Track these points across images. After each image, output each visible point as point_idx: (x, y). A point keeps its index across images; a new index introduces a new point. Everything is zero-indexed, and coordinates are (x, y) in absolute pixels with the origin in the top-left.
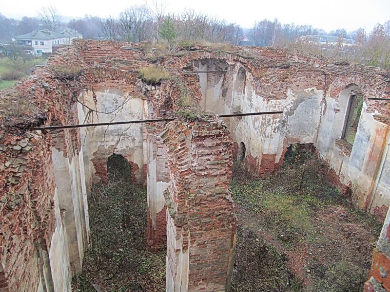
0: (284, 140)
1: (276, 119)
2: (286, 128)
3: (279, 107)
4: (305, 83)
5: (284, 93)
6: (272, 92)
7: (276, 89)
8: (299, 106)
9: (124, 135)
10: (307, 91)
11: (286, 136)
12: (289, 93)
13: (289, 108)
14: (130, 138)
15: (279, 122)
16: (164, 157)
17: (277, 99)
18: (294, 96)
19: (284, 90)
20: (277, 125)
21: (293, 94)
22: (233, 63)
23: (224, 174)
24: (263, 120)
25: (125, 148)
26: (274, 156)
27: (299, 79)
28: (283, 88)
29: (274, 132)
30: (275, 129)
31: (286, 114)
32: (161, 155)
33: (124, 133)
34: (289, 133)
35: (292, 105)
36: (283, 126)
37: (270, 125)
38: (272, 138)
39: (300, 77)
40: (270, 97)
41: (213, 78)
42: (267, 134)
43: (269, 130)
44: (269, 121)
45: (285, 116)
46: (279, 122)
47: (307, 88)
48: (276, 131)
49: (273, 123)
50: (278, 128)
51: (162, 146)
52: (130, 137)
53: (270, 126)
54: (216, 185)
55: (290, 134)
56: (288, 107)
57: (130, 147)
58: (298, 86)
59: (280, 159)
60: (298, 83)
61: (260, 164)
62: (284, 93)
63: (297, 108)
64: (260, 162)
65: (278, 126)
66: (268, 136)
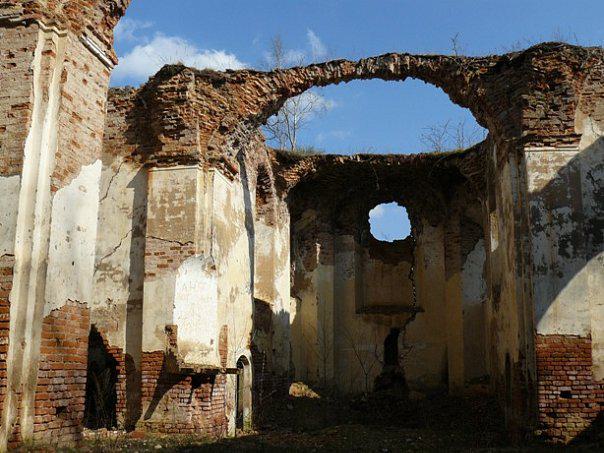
1: (560, 210)
5: (566, 127)
9: (106, 265)
14: (118, 277)
15: (574, 217)
19: (564, 116)
20: (569, 228)
24: (517, 218)
25: (104, 305)
28: (556, 108)
29: (562, 252)
30: (563, 245)
33: (104, 261)
37: (540, 228)
41: (456, 248)
42: (537, 261)
44: (536, 214)
45: (594, 204)
46: (574, 217)
48: (570, 250)
49: (551, 224)
50: (574, 238)
52: (118, 272)
57: (115, 302)
62: (566, 127)
66: (543, 270)
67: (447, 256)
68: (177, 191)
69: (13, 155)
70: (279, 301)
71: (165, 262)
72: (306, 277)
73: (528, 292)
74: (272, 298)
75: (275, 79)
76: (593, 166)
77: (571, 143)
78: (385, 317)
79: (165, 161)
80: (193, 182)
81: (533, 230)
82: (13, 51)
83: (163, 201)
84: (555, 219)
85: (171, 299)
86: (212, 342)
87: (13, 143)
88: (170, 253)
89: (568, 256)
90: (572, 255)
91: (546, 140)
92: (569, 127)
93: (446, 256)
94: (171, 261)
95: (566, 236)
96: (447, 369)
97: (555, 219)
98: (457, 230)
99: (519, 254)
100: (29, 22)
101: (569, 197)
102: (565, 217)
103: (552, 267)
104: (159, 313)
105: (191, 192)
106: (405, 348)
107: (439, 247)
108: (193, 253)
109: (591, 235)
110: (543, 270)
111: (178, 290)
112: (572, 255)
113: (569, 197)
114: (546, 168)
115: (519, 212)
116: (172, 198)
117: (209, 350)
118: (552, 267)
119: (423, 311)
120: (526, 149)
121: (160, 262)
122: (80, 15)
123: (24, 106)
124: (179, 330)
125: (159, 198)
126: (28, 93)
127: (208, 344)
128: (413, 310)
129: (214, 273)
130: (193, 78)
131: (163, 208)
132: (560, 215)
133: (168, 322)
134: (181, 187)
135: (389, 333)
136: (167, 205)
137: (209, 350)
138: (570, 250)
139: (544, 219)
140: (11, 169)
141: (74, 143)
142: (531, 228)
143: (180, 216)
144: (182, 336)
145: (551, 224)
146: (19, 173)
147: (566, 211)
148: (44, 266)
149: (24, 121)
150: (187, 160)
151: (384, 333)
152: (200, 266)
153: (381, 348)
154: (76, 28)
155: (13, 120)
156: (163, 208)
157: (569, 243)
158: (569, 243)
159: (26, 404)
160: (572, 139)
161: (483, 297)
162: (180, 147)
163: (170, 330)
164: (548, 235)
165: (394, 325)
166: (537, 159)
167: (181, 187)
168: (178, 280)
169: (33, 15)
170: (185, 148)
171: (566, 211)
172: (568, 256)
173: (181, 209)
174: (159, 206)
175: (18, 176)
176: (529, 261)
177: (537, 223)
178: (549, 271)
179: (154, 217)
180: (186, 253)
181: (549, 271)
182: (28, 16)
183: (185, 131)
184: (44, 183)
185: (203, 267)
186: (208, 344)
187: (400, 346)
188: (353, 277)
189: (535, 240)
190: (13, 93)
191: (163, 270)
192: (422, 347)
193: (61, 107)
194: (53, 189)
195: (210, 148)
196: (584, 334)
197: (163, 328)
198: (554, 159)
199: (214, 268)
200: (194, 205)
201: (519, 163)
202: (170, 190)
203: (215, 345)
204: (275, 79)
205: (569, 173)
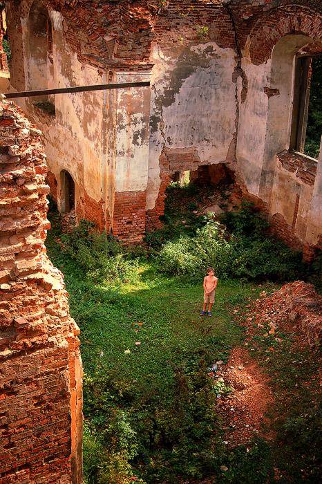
0: (161, 161)
2: (163, 134)
10: (197, 52)
11: (163, 152)
13: (163, 90)
15: (143, 120)
17: (132, 70)
19: (144, 50)
20: (140, 126)
21: (167, 59)
23: (32, 229)
24: (105, 116)
26: (142, 197)
27: (173, 24)
29: (135, 142)
30: (136, 137)
31: (157, 102)
34: (170, 144)
36: (154, 129)
37: (122, 127)
38: (132, 156)
39: (177, 21)
42: (119, 148)
47: (197, 44)
48: (139, 140)
49: (129, 124)
50: (143, 133)
53: (123, 131)
54: (16, 254)
55: (172, 147)
59: (157, 201)
65: (143, 131)
66: (122, 153)
73: (110, 165)
77: (147, 69)
84: (132, 121)
89: (138, 145)
90: (140, 143)
91: (132, 68)
92: (146, 57)
95: (138, 132)
97: (132, 121)
99: (105, 140)
103: (127, 152)
110: (122, 153)
112: (140, 143)
113: (142, 106)
115: (107, 112)
118: (127, 152)
132: (136, 119)
145: (129, 124)
147: (139, 115)
157: (139, 136)
158: (139, 136)
160: (148, 67)
164: (127, 131)
171: (139, 115)
172: (138, 145)
178: (126, 154)
181: (126, 154)
189: (119, 135)
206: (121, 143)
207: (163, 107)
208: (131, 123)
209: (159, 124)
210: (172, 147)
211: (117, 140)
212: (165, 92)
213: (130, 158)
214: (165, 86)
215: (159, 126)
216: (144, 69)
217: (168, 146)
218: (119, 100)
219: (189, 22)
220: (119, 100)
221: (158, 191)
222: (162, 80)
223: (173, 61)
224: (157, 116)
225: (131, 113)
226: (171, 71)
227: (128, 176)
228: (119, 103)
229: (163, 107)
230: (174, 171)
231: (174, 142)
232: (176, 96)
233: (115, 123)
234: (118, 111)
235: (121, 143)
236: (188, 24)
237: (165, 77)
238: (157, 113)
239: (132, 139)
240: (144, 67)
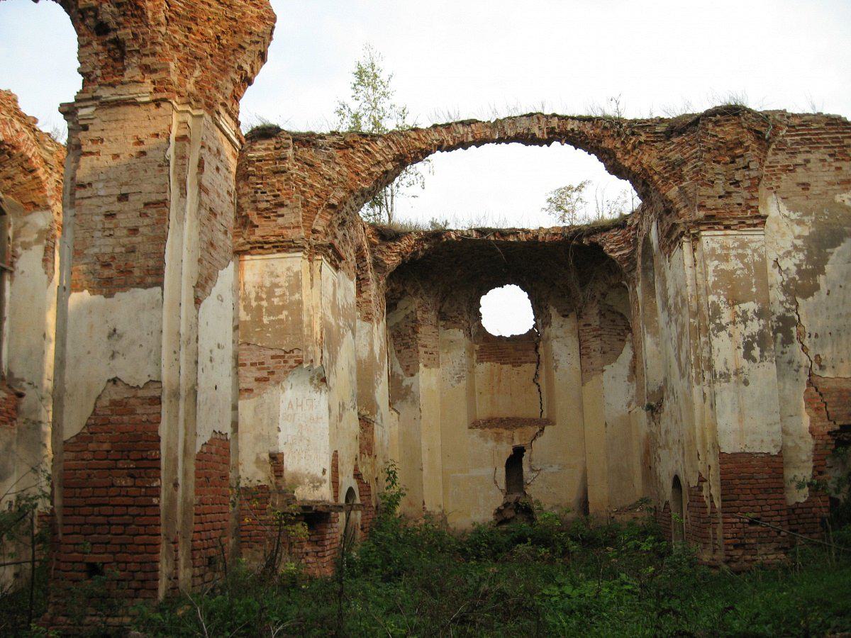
1: (744, 306)
2: (804, 348)
3: (741, 257)
4: (830, 176)
6: (702, 206)
7: (710, 192)
8: (832, 258)
11: (810, 383)
12: (773, 208)
13: (794, 269)
15: (760, 314)
16: (102, 193)
17: (727, 227)
18: (800, 223)
19: (746, 194)
20: (755, 326)
21: (794, 216)
22: (626, 251)
26: (775, 464)
27: (799, 159)
28: (736, 183)
29: (748, 356)
30: (748, 347)
31: (785, 289)
32: (90, 184)
34: (822, 367)
35: (801, 256)
36: (788, 340)
37: (721, 328)
38: (746, 383)
39: (805, 156)
40: (698, 223)
41: (595, 344)
42: (719, 367)
43: (725, 350)
44: (717, 312)
45: (782, 298)
46: (760, 314)
48: (756, 352)
49: (734, 323)
50: (762, 339)
51: (94, 148)
53: (723, 334)
55: (828, 374)
56: (786, 264)
58: (805, 186)
60: (801, 176)
61: (718, 504)
63: (828, 268)
64: (715, 491)
66: (726, 376)
67: (584, 353)
68: (276, 285)
69: (151, 263)
70: (379, 417)
71: (265, 374)
72: (404, 384)
74: (372, 413)
75: (390, 143)
76: (781, 253)
77: (755, 225)
78: (506, 433)
79: (261, 247)
80: (297, 275)
81: (713, 330)
82: (142, 137)
83: (258, 298)
84: (738, 316)
85: (274, 420)
86: (324, 472)
87: (149, 248)
88: (270, 363)
89: (754, 360)
90: (758, 359)
91: (726, 223)
92: (753, 207)
93: (581, 355)
94: (273, 373)
95: (752, 337)
96: (585, 492)
97: (738, 316)
98: (595, 321)
99: (698, 359)
100: (157, 103)
101: (754, 290)
102: (750, 314)
103: (736, 374)
104: (259, 438)
105: (296, 286)
106: (532, 470)
107: (573, 343)
108: (300, 363)
109: (780, 335)
110: (726, 376)
111: (283, 407)
112: (758, 359)
113: (754, 290)
114: (727, 256)
116: (270, 293)
117: (321, 482)
118: (736, 374)
119: (554, 424)
120: (703, 233)
121: (258, 374)
122: (214, 91)
123: (164, 203)
124: (285, 457)
125: (253, 295)
126: (165, 187)
127: (320, 474)
128: (542, 423)
129: (323, 387)
130: (290, 142)
131: (259, 308)
132: (745, 312)
133: (272, 449)
134: (282, 280)
135: (510, 451)
136: (264, 303)
137: (321, 482)
138: (756, 352)
139: (726, 316)
140: (149, 280)
141: (212, 245)
142: (711, 327)
143: (282, 316)
144: (290, 465)
145: (734, 323)
146: (160, 284)
147: (751, 306)
148: (193, 392)
149: (163, 221)
150: (284, 246)
151: (506, 450)
152: (307, 379)
153: (502, 471)
154: (210, 107)
155: (147, 221)
156: (259, 308)
157: (755, 345)
158: (755, 345)
159: (182, 555)
160: (756, 221)
161: (629, 405)
162: (278, 231)
163: (276, 460)
164: (730, 336)
165: (517, 443)
166: (717, 246)
167: (282, 280)
168: (282, 397)
169: (164, 95)
170: (284, 232)
171: (751, 306)
172: (754, 360)
173: (283, 308)
174: (254, 304)
175: (159, 289)
176: (710, 367)
177: (718, 321)
179: (248, 318)
180: (291, 362)
181: (733, 378)
182: (159, 96)
183: (281, 211)
184: (187, 295)
185: (312, 379)
186: (320, 474)
187: (526, 469)
188: (463, 382)
189: (716, 342)
190: (147, 187)
191: (262, 384)
192: (552, 470)
193: (200, 205)
194: (198, 302)
195: (314, 231)
196: (774, 452)
197: (266, 456)
198: (736, 245)
199: (324, 380)
200: (300, 302)
201: (694, 250)
202: (268, 284)
203: (328, 476)
204: (390, 143)
205: (754, 263)
206: (722, 357)
207: (799, 300)
208: (738, 319)
209: (794, 329)
210: (828, 374)
211: (715, 352)
212: (799, 272)
213: (742, 386)
214: (798, 262)
215: (795, 334)
216: (749, 226)
217: (818, 372)
218: (711, 279)
219: (827, 157)
220: (711, 279)
221: (811, 464)
222: (789, 253)
223: (806, 219)
224: (789, 315)
225: (733, 301)
226: (805, 237)
227: (740, 421)
228: (710, 284)
229: (799, 300)
230: (838, 423)
231: (829, 364)
232: (821, 279)
233: (707, 322)
234: (712, 298)
235: (722, 357)
236: (824, 160)
237: (795, 247)
238: (788, 310)
239: (742, 350)
240: (748, 222)
